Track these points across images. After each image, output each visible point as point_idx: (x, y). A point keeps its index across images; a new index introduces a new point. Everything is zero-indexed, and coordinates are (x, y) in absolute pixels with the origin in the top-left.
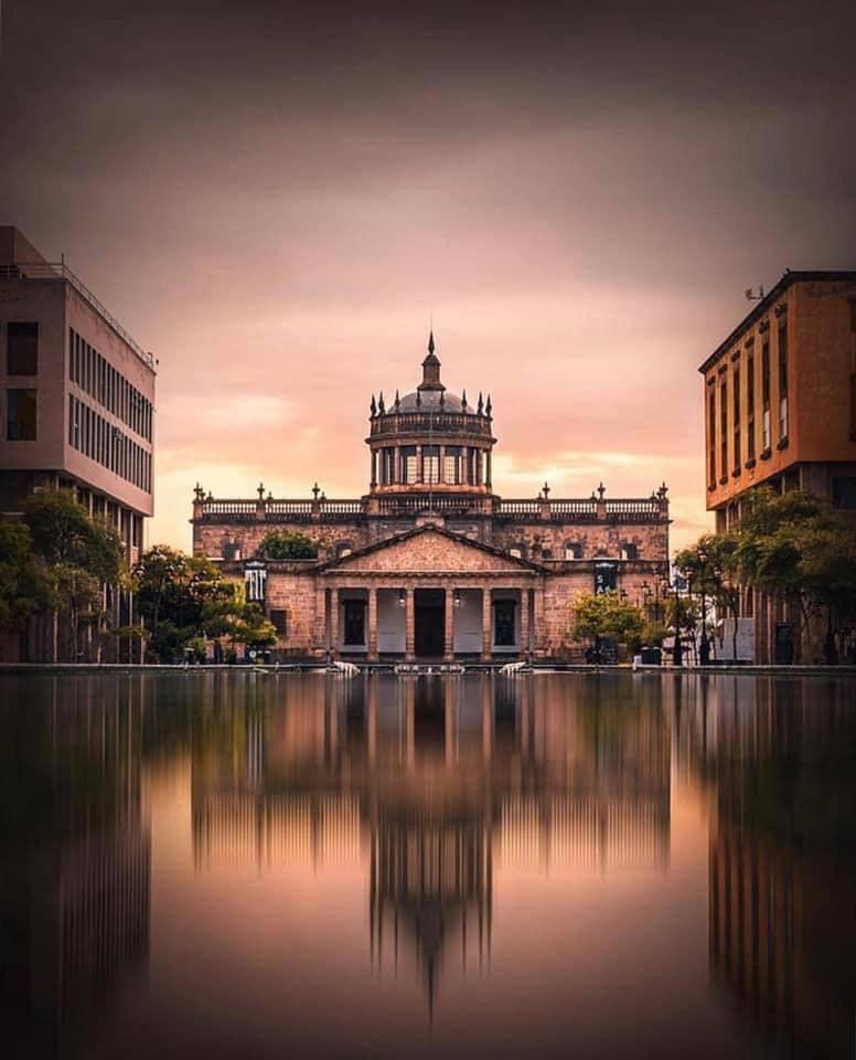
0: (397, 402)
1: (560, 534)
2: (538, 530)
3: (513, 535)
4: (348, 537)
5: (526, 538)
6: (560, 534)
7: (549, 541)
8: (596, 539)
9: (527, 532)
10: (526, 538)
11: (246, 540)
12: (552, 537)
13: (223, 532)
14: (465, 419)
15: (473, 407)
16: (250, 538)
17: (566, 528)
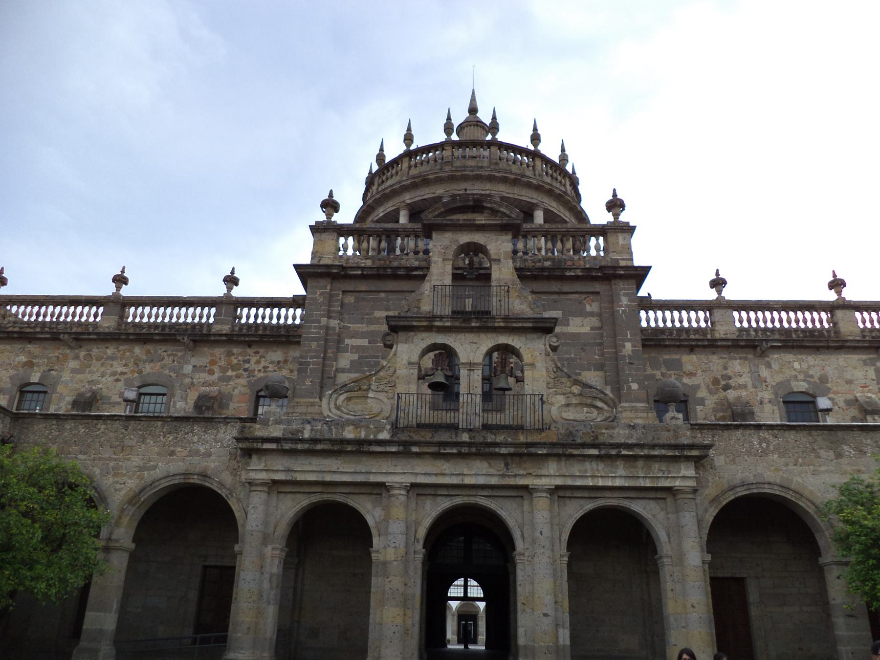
0: (408, 138)
1: (764, 373)
2: (715, 362)
3: (658, 374)
4: (285, 372)
5: (686, 380)
6: (764, 373)
7: (744, 387)
8: (849, 382)
9: (688, 368)
10: (686, 380)
11: (66, 376)
12: (745, 379)
13: (23, 358)
14: (538, 162)
15: (550, 150)
16: (74, 371)
17: (775, 358)
